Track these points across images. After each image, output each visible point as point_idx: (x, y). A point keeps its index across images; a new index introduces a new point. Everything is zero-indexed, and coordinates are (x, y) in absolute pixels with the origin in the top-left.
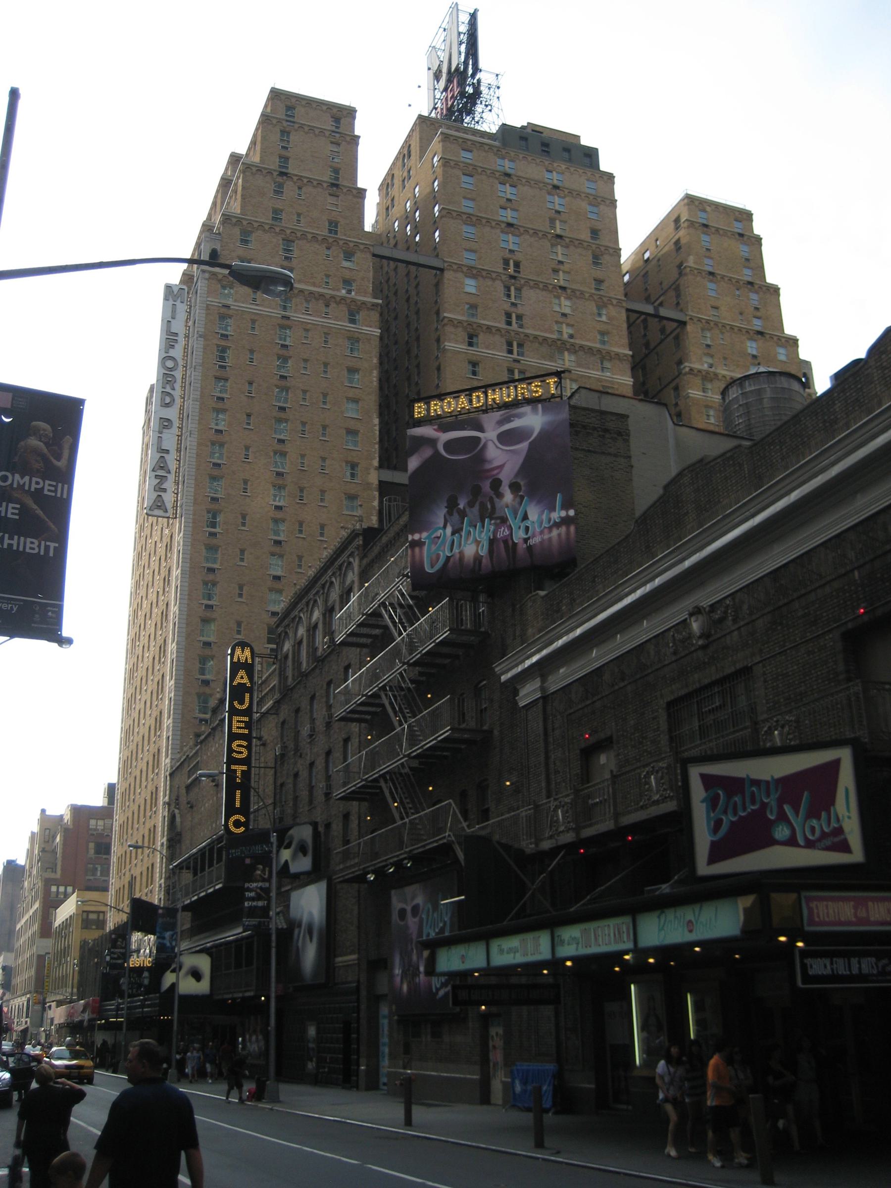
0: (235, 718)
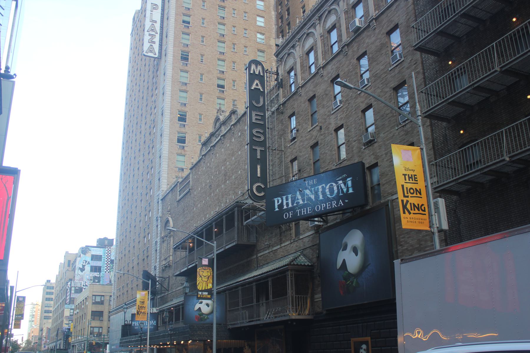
0: (254, 114)
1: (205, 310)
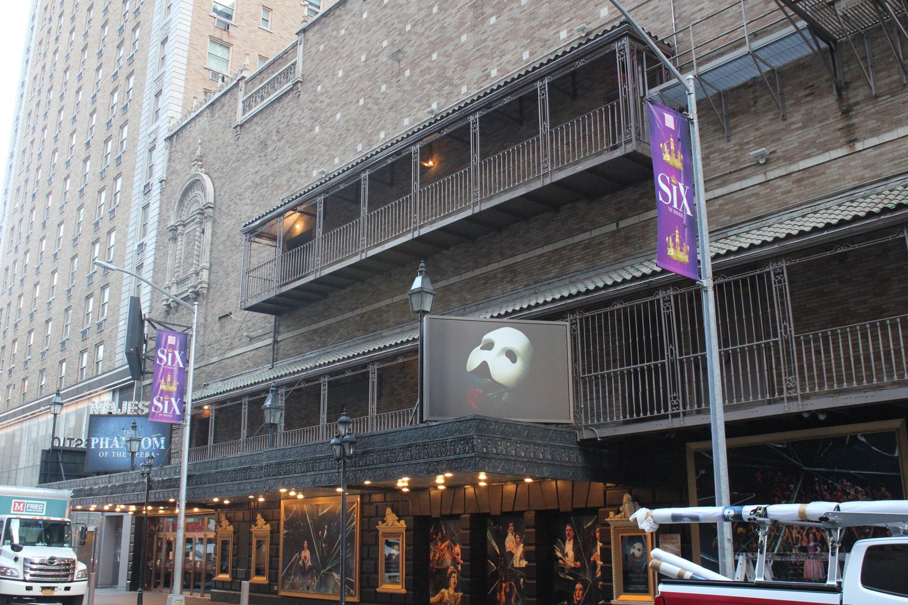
1: (504, 371)
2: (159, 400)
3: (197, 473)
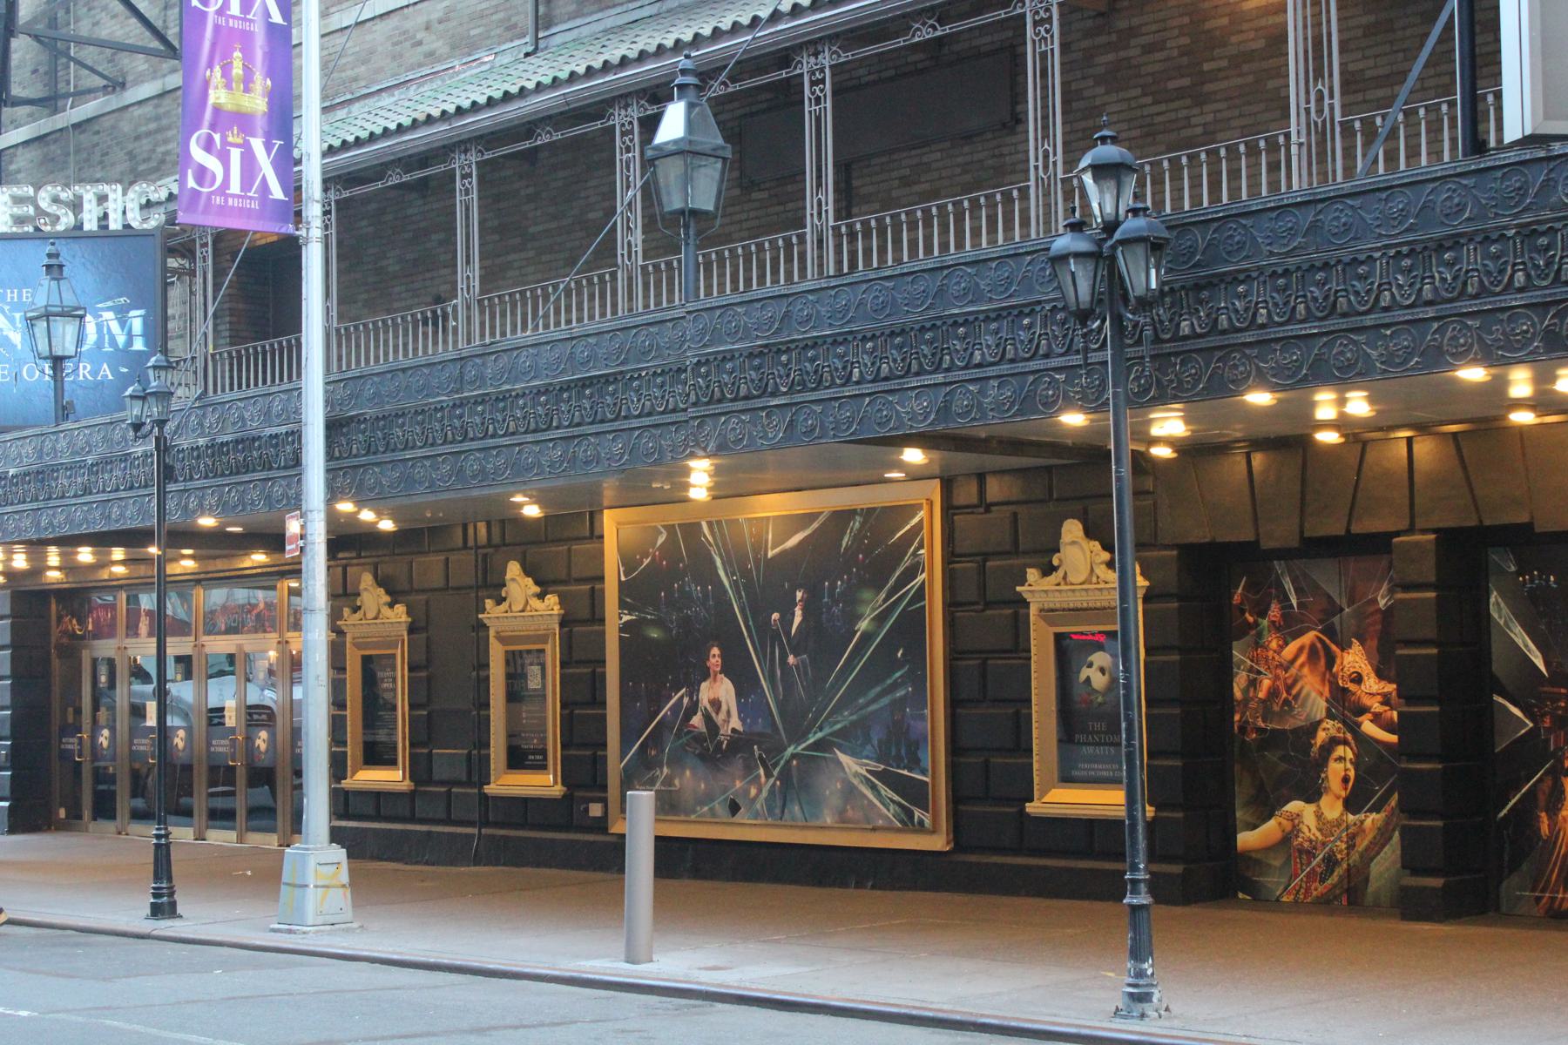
2: (208, 146)
3: (370, 412)
